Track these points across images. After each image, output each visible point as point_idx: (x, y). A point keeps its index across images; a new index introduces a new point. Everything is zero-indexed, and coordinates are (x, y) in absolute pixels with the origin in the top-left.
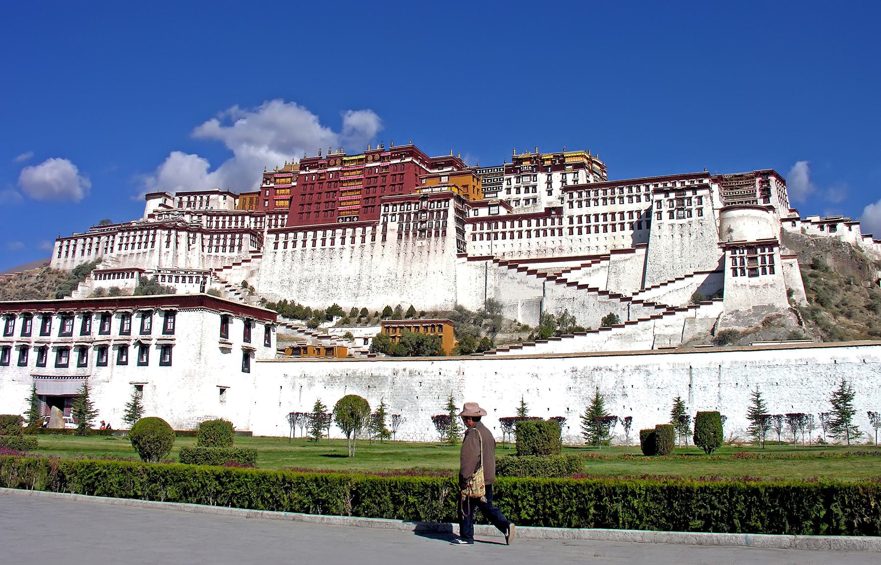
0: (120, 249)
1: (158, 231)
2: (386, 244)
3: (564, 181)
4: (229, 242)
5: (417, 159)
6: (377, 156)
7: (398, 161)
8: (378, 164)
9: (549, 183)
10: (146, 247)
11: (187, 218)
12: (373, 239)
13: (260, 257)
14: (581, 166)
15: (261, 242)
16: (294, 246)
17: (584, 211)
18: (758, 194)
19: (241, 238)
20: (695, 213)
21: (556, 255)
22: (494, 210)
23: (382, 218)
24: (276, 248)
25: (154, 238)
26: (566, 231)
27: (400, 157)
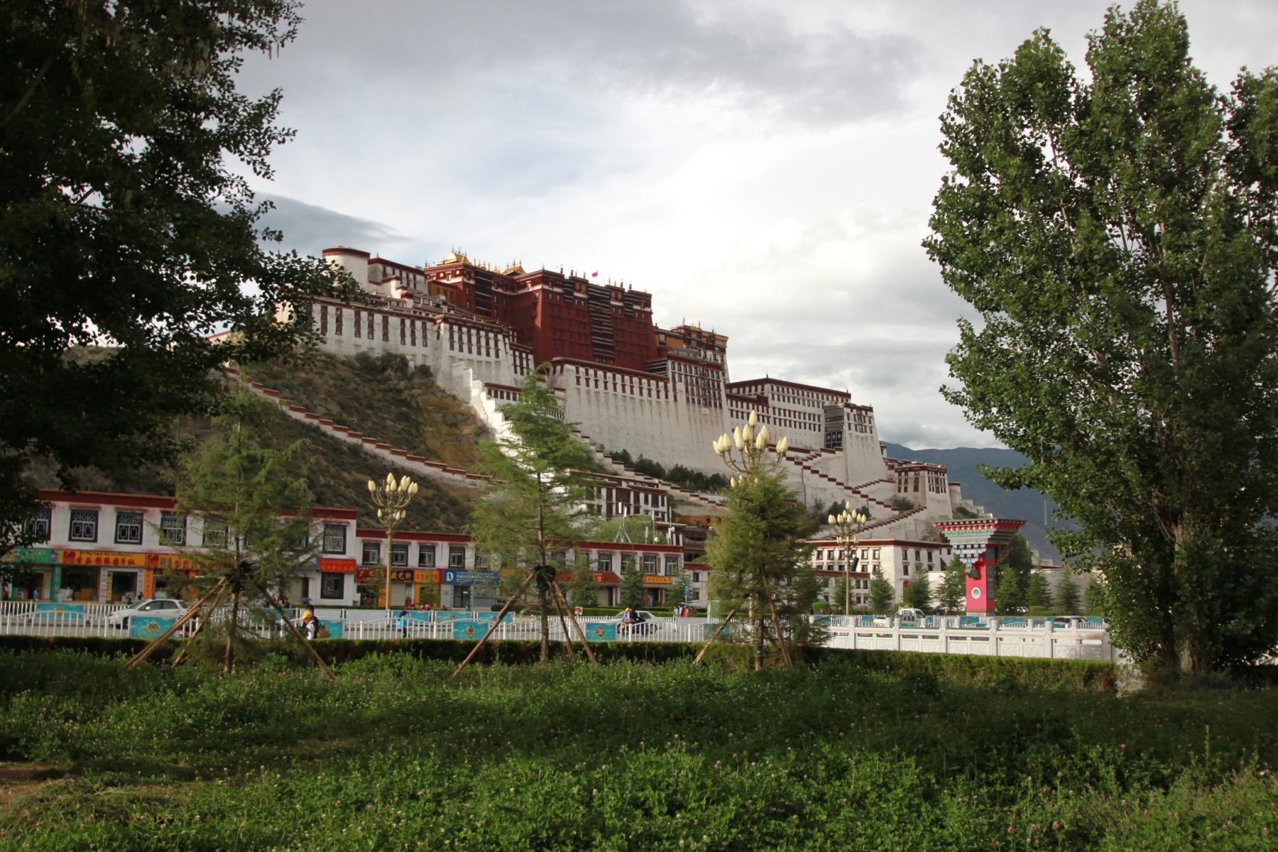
0: (452, 348)
6: (620, 296)
10: (488, 354)
16: (596, 386)
23: (670, 376)
24: (578, 383)
26: (772, 420)
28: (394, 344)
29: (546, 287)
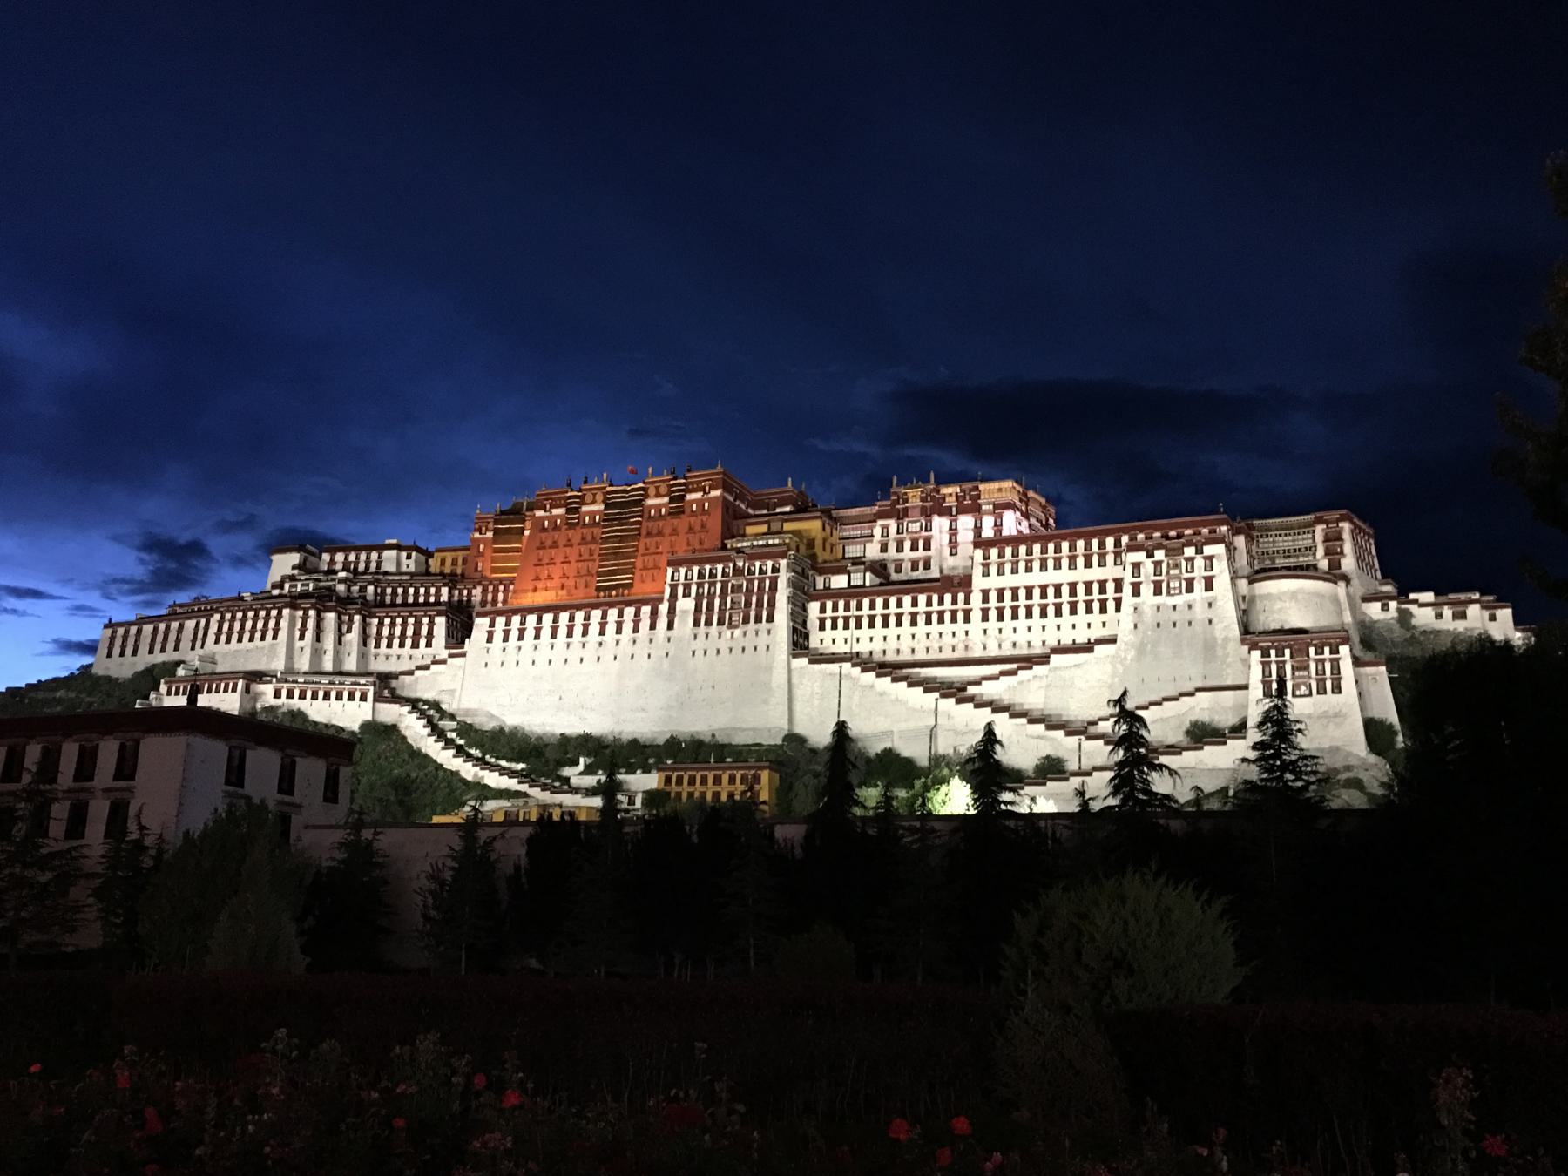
0: (217, 642)
1: (286, 612)
2: (670, 633)
3: (978, 530)
4: (410, 632)
5: (731, 493)
6: (663, 490)
7: (698, 495)
8: (666, 499)
9: (953, 531)
11: (341, 588)
12: (653, 627)
13: (463, 655)
14: (1010, 506)
15: (467, 631)
17: (1008, 580)
18: (1320, 552)
19: (431, 623)
20: (1199, 586)
21: (960, 654)
22: (857, 579)
24: (489, 640)
25: (277, 623)
26: (976, 615)
27: (703, 490)
28: (185, 653)
29: (540, 513)
